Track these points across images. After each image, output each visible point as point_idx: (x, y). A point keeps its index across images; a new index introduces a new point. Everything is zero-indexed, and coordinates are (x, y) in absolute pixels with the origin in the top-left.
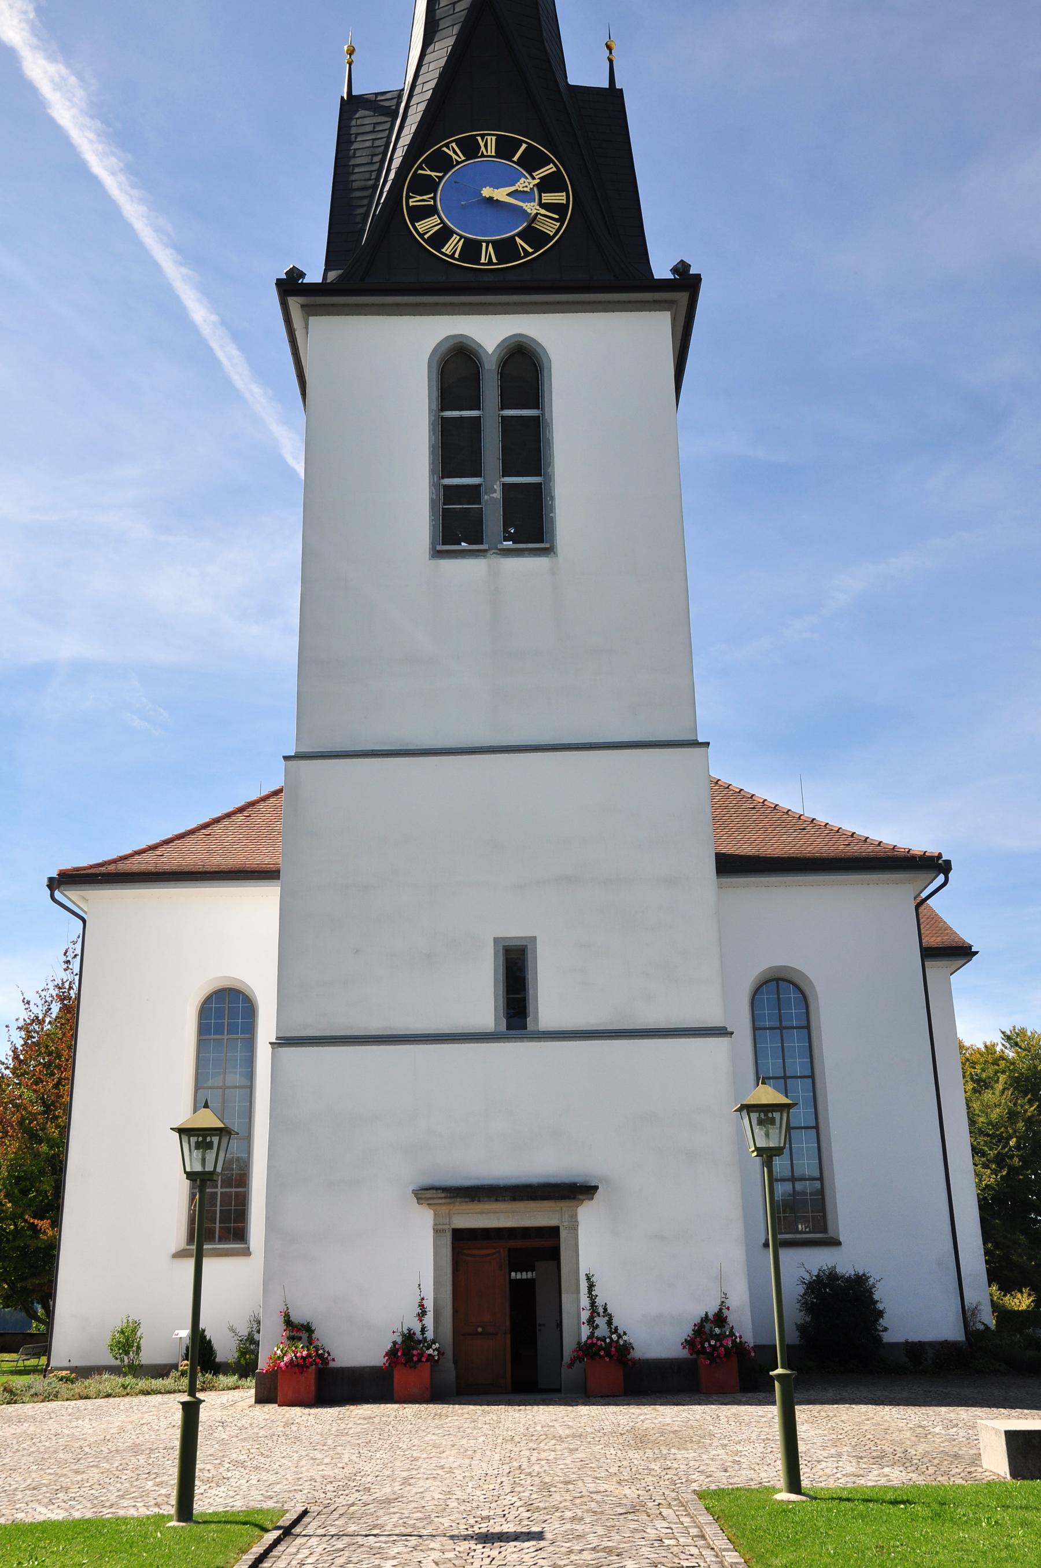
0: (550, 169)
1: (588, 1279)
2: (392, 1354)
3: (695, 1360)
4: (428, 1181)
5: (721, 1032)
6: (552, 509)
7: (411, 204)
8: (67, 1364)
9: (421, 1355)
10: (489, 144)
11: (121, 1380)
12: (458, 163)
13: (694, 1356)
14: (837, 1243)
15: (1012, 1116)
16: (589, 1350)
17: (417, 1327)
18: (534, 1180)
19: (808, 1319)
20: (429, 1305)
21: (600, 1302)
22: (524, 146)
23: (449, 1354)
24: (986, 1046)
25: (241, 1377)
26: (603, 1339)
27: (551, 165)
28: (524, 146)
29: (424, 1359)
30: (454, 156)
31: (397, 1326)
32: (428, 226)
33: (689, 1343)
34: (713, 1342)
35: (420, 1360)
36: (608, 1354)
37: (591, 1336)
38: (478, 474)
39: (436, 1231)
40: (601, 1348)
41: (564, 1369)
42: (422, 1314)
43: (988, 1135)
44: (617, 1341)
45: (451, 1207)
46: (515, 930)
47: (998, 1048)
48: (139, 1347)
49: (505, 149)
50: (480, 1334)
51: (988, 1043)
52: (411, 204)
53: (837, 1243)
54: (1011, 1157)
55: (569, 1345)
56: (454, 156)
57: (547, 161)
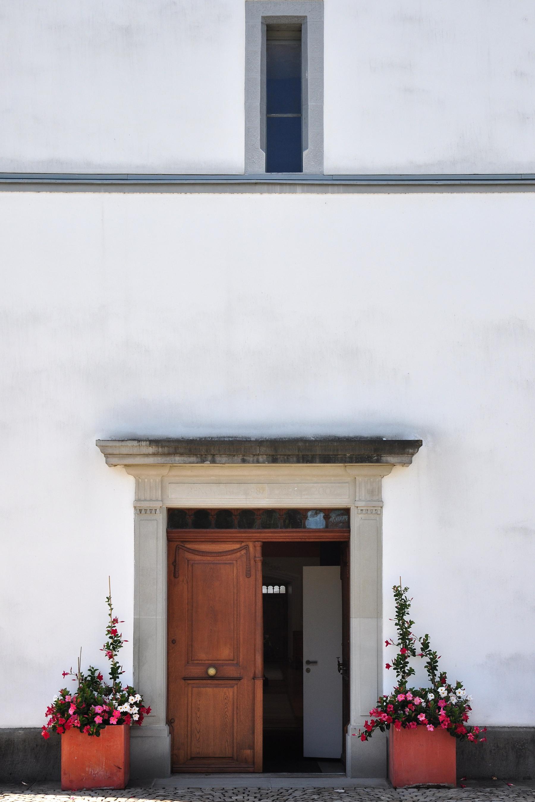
1: (398, 594)
2: (59, 710)
9: (110, 713)
16: (396, 713)
17: (104, 667)
20: (126, 631)
21: (417, 632)
23: (159, 710)
26: (423, 694)
29: (113, 721)
31: (71, 665)
35: (106, 722)
36: (433, 720)
37: (401, 689)
39: (139, 511)
40: (419, 710)
41: (352, 741)
42: (114, 644)
44: (447, 698)
45: (165, 471)
46: (284, 4)
50: (212, 678)
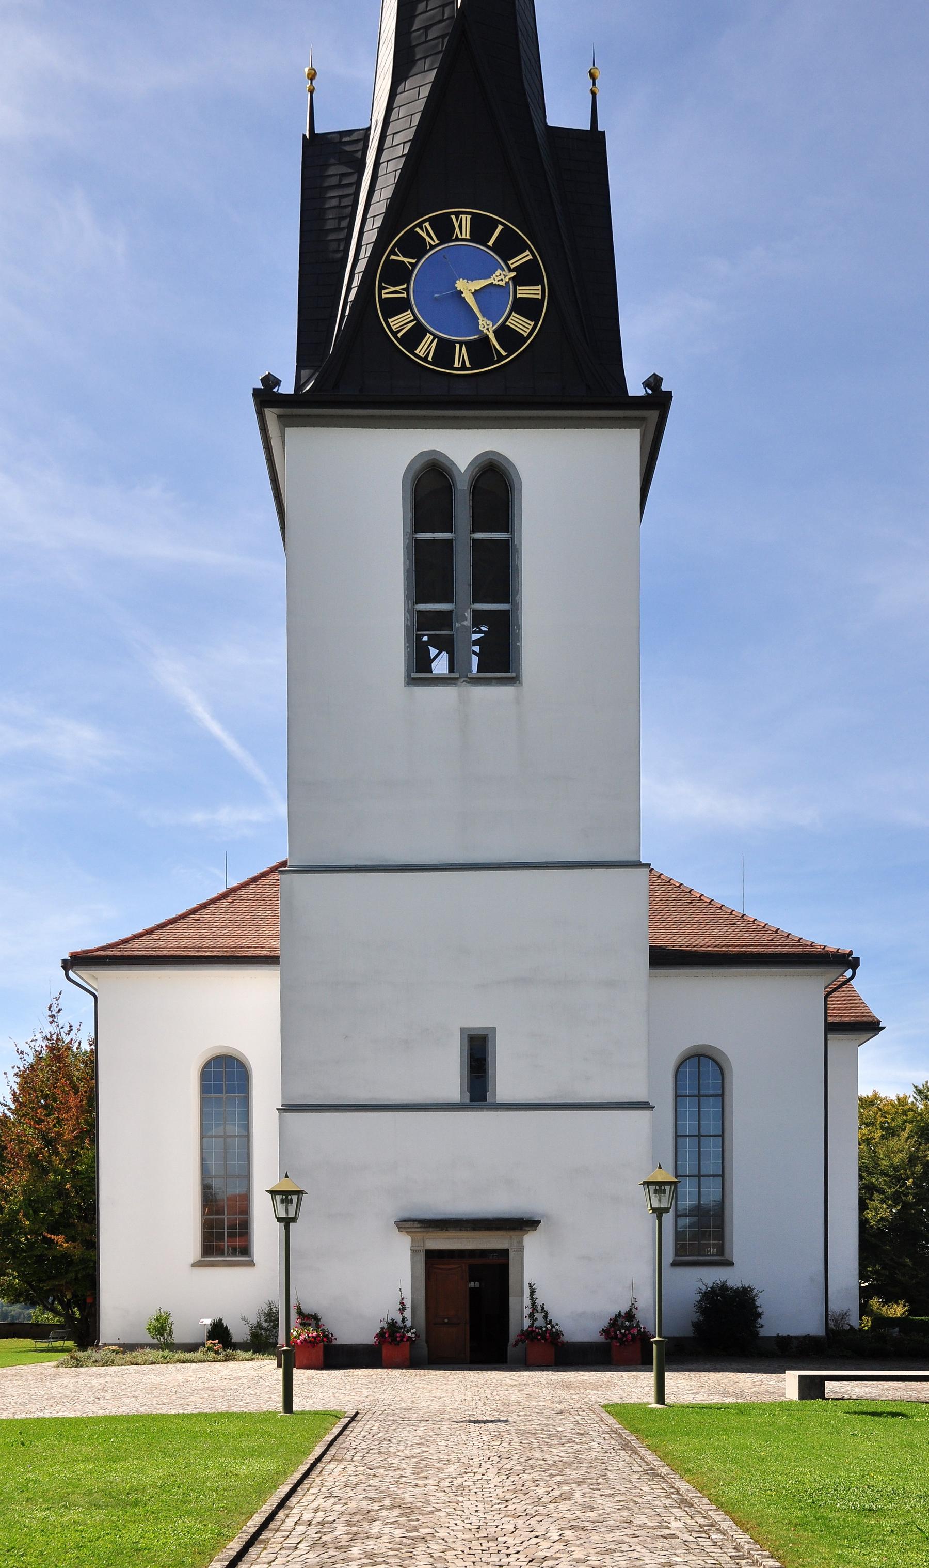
0: (525, 257)
1: (531, 1286)
2: (381, 1335)
3: (609, 1344)
4: (407, 1215)
5: (645, 1106)
6: (518, 638)
7: (384, 296)
8: (117, 1342)
10: (463, 226)
11: (161, 1353)
12: (432, 247)
13: (609, 1341)
14: (732, 1264)
15: (913, 1160)
16: (530, 1335)
17: (398, 1318)
18: (489, 1216)
19: (701, 1318)
20: (408, 1303)
22: (500, 227)
24: (898, 1099)
25: (254, 1352)
26: (541, 1328)
27: (527, 252)
28: (500, 227)
30: (428, 239)
32: (401, 322)
33: (605, 1332)
34: (623, 1331)
35: (402, 1340)
37: (532, 1325)
38: (449, 599)
39: (413, 1251)
40: (538, 1334)
42: (403, 1308)
43: (890, 1176)
47: (910, 1100)
48: (171, 1332)
49: (481, 230)
51: (901, 1096)
52: (384, 296)
53: (732, 1264)
54: (906, 1195)
55: (514, 1332)
56: (428, 239)
57: (523, 247)
